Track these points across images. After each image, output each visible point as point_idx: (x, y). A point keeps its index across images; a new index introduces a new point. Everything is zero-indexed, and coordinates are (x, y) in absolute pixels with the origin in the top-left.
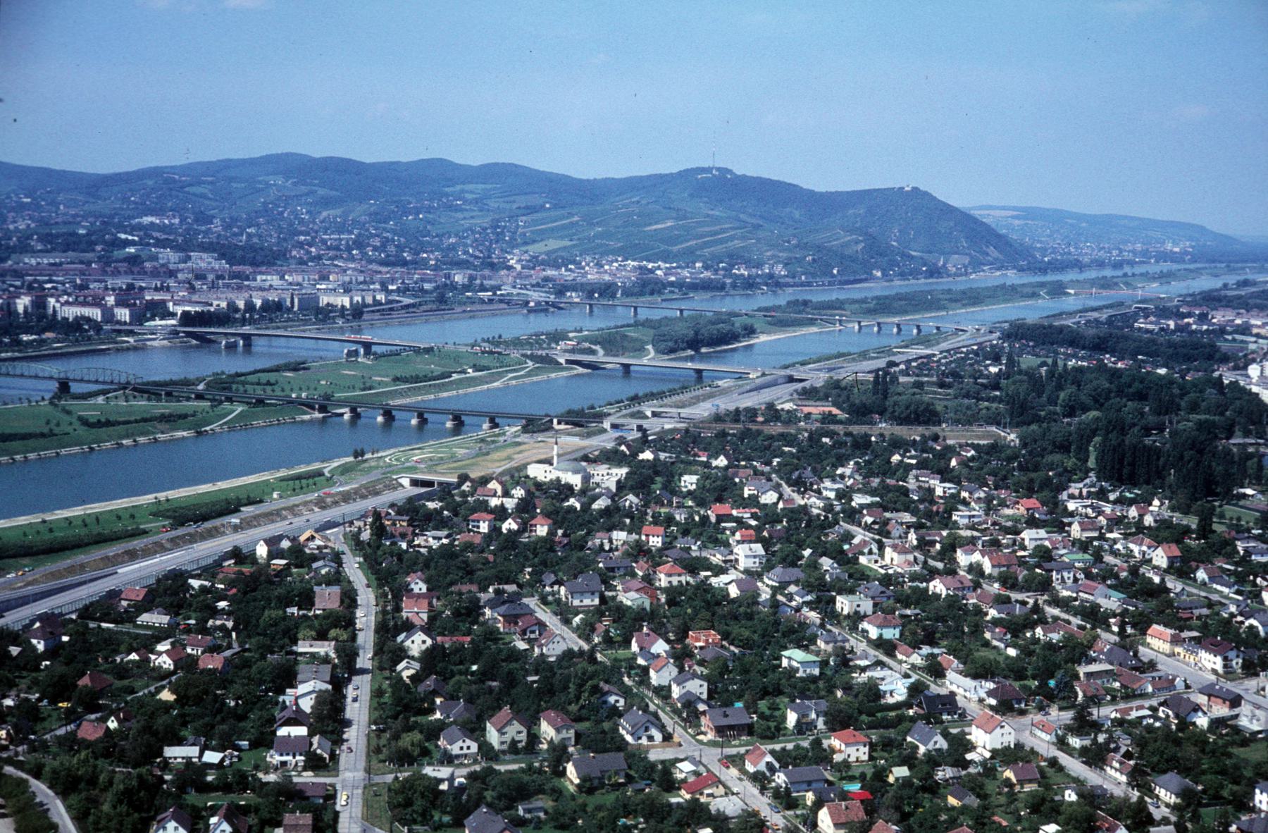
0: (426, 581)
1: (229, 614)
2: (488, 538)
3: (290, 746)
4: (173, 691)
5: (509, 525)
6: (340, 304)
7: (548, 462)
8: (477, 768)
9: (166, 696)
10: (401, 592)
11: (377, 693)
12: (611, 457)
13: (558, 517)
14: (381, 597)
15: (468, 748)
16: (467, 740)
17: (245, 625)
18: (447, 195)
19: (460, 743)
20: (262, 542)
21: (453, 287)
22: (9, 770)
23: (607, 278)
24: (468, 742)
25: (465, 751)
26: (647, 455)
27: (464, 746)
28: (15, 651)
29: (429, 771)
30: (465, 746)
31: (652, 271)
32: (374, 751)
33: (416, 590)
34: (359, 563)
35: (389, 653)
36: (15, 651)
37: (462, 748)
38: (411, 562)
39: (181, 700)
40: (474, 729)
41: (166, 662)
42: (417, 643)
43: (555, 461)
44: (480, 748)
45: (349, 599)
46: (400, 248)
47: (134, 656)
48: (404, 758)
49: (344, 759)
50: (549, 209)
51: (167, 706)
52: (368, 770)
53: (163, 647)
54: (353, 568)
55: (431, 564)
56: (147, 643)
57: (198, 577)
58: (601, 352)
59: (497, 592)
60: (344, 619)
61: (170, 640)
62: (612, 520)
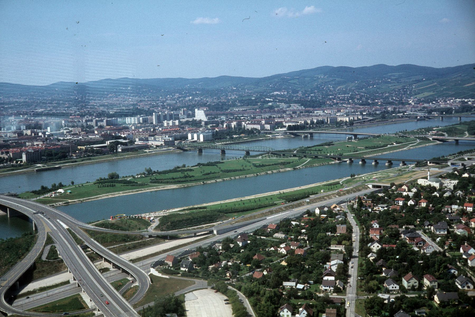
0: (378, 224)
1: (306, 234)
2: (402, 207)
3: (328, 283)
4: (286, 262)
5: (411, 203)
6: (345, 120)
7: (426, 178)
8: (399, 295)
9: (284, 263)
10: (369, 227)
11: (360, 265)
12: (451, 176)
13: (430, 199)
14: (361, 229)
15: (395, 287)
16: (395, 284)
17: (311, 239)
18: (385, 78)
19: (392, 285)
20: (317, 208)
21: (388, 112)
22: (230, 287)
23: (448, 106)
24: (395, 285)
25: (394, 289)
26: (466, 175)
27: (394, 287)
28: (232, 246)
29: (380, 295)
30: (394, 286)
31: (467, 102)
32: (359, 287)
33: (375, 227)
34: (353, 216)
35: (365, 251)
36: (232, 246)
37: (393, 287)
38: (374, 216)
39: (289, 265)
40: (398, 281)
41: (283, 251)
42: (376, 247)
43: (429, 178)
44: (400, 288)
45: (350, 230)
46: (367, 99)
47: (272, 249)
48: (371, 290)
49: (348, 289)
50: (425, 80)
51: (284, 267)
52: (357, 294)
53: (283, 246)
54: (351, 218)
55: (381, 217)
56: (277, 244)
57: (295, 221)
58: (446, 135)
59: (406, 228)
60: (348, 237)
61: (285, 243)
62: (452, 200)
